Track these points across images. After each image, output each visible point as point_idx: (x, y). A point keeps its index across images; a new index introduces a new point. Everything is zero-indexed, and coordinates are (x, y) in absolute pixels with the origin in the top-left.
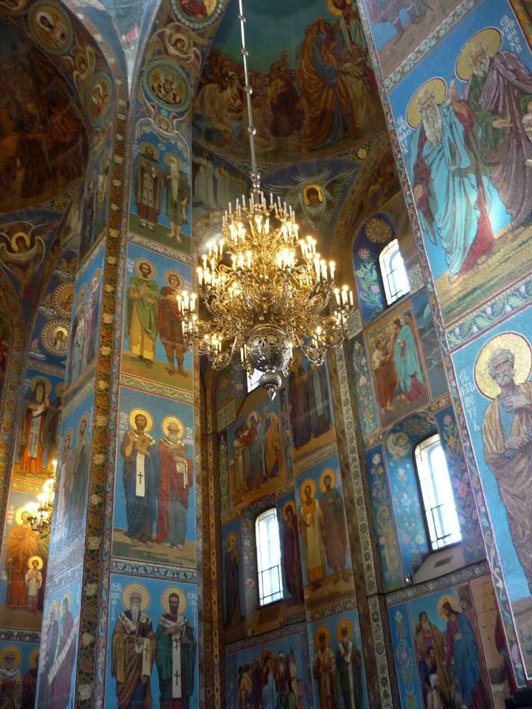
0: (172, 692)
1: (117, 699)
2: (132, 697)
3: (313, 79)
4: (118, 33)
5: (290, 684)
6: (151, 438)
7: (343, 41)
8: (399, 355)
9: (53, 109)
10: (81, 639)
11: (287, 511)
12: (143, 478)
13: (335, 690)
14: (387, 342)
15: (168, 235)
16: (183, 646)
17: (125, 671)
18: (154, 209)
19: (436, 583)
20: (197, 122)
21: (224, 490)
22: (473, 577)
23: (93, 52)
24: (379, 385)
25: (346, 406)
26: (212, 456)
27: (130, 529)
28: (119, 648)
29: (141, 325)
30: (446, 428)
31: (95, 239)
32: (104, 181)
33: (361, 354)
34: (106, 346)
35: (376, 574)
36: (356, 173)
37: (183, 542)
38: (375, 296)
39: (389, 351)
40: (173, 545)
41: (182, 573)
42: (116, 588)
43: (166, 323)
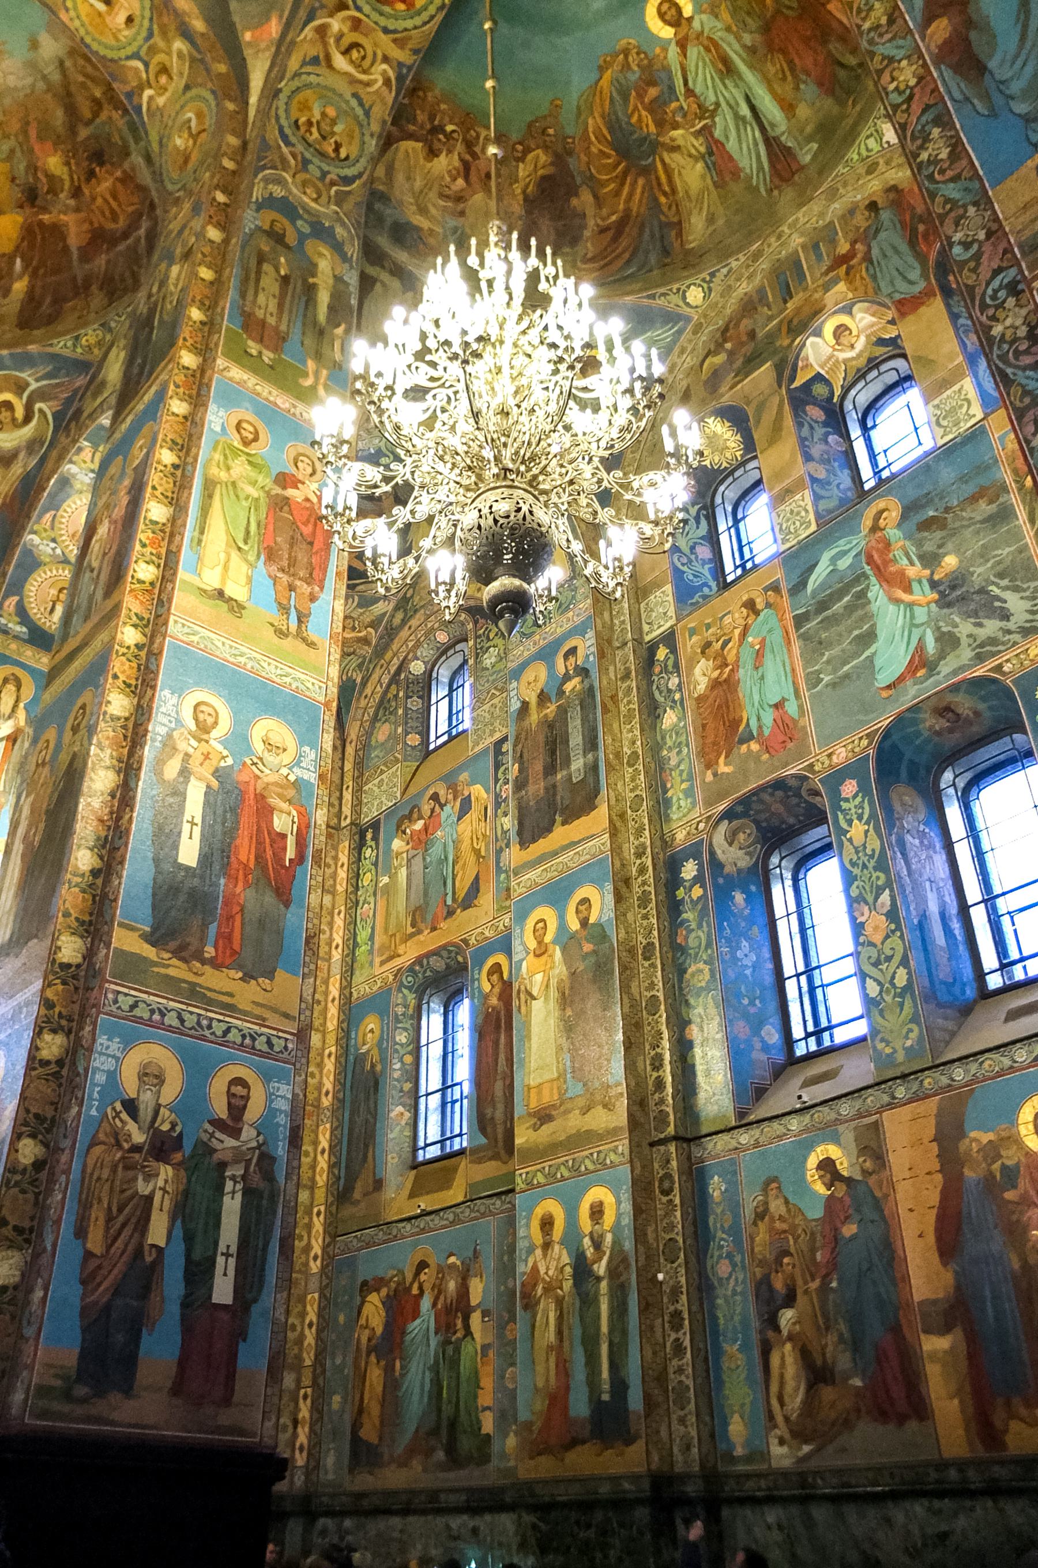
0: (211, 1289)
1: (78, 1289)
2: (117, 1291)
3: (609, 157)
4: (239, 27)
5: (466, 1319)
6: (225, 753)
7: (672, 88)
8: (750, 666)
9: (97, 169)
10: (13, 1149)
11: (490, 974)
12: (197, 831)
13: (566, 1333)
14: (726, 643)
15: (301, 381)
16: (247, 1192)
17: (107, 1229)
18: (276, 329)
19: (806, 1119)
20: (377, 206)
21: (363, 935)
22: (889, 1106)
23: (185, 52)
24: (704, 726)
25: (630, 765)
26: (345, 868)
27: (155, 929)
28: (99, 1179)
29: (228, 532)
30: (844, 805)
31: (151, 374)
32: (179, 275)
33: (670, 668)
34: (147, 563)
35: (673, 1098)
36: (680, 332)
37: (270, 975)
38: (703, 565)
39: (731, 658)
40: (248, 977)
41: (264, 1039)
42: (108, 1048)
43: (279, 539)
